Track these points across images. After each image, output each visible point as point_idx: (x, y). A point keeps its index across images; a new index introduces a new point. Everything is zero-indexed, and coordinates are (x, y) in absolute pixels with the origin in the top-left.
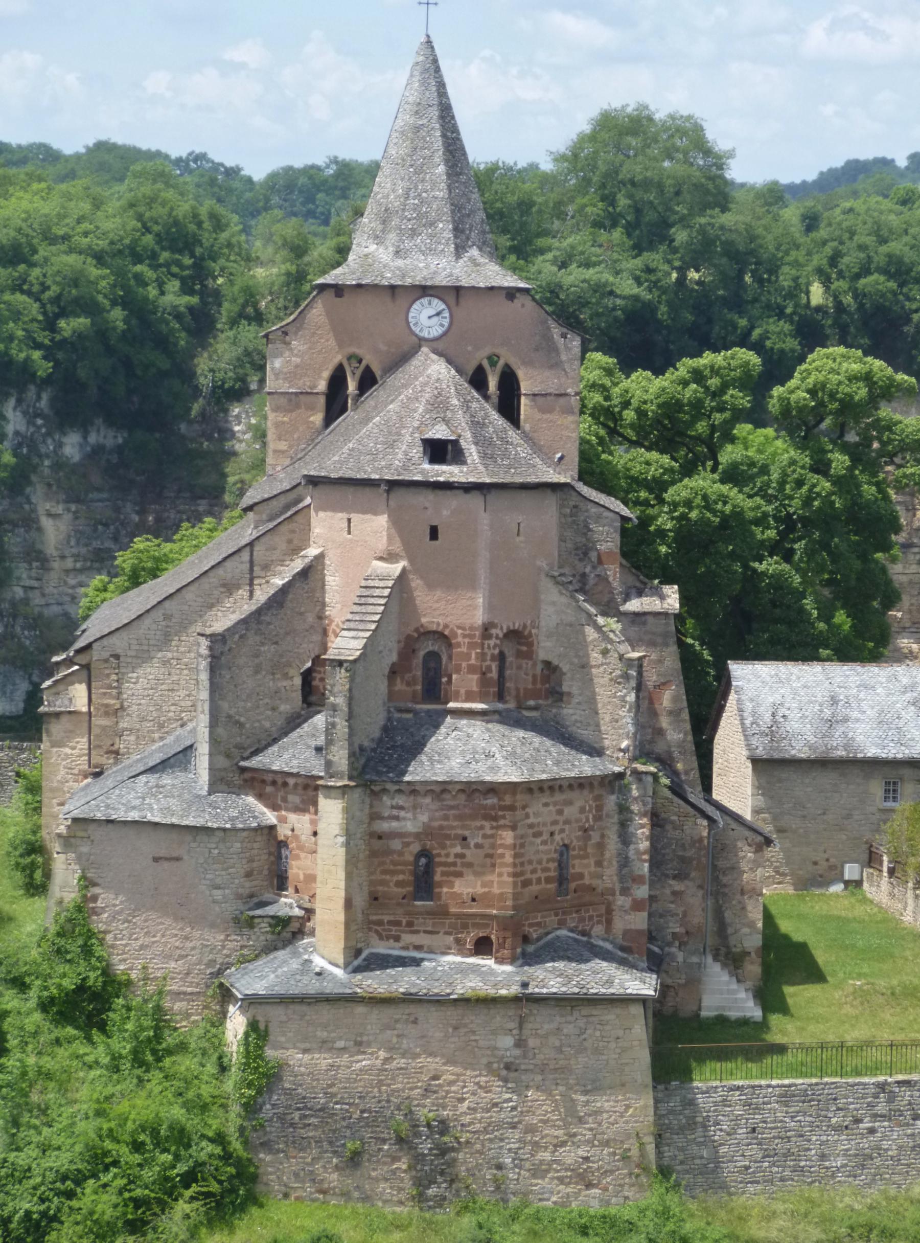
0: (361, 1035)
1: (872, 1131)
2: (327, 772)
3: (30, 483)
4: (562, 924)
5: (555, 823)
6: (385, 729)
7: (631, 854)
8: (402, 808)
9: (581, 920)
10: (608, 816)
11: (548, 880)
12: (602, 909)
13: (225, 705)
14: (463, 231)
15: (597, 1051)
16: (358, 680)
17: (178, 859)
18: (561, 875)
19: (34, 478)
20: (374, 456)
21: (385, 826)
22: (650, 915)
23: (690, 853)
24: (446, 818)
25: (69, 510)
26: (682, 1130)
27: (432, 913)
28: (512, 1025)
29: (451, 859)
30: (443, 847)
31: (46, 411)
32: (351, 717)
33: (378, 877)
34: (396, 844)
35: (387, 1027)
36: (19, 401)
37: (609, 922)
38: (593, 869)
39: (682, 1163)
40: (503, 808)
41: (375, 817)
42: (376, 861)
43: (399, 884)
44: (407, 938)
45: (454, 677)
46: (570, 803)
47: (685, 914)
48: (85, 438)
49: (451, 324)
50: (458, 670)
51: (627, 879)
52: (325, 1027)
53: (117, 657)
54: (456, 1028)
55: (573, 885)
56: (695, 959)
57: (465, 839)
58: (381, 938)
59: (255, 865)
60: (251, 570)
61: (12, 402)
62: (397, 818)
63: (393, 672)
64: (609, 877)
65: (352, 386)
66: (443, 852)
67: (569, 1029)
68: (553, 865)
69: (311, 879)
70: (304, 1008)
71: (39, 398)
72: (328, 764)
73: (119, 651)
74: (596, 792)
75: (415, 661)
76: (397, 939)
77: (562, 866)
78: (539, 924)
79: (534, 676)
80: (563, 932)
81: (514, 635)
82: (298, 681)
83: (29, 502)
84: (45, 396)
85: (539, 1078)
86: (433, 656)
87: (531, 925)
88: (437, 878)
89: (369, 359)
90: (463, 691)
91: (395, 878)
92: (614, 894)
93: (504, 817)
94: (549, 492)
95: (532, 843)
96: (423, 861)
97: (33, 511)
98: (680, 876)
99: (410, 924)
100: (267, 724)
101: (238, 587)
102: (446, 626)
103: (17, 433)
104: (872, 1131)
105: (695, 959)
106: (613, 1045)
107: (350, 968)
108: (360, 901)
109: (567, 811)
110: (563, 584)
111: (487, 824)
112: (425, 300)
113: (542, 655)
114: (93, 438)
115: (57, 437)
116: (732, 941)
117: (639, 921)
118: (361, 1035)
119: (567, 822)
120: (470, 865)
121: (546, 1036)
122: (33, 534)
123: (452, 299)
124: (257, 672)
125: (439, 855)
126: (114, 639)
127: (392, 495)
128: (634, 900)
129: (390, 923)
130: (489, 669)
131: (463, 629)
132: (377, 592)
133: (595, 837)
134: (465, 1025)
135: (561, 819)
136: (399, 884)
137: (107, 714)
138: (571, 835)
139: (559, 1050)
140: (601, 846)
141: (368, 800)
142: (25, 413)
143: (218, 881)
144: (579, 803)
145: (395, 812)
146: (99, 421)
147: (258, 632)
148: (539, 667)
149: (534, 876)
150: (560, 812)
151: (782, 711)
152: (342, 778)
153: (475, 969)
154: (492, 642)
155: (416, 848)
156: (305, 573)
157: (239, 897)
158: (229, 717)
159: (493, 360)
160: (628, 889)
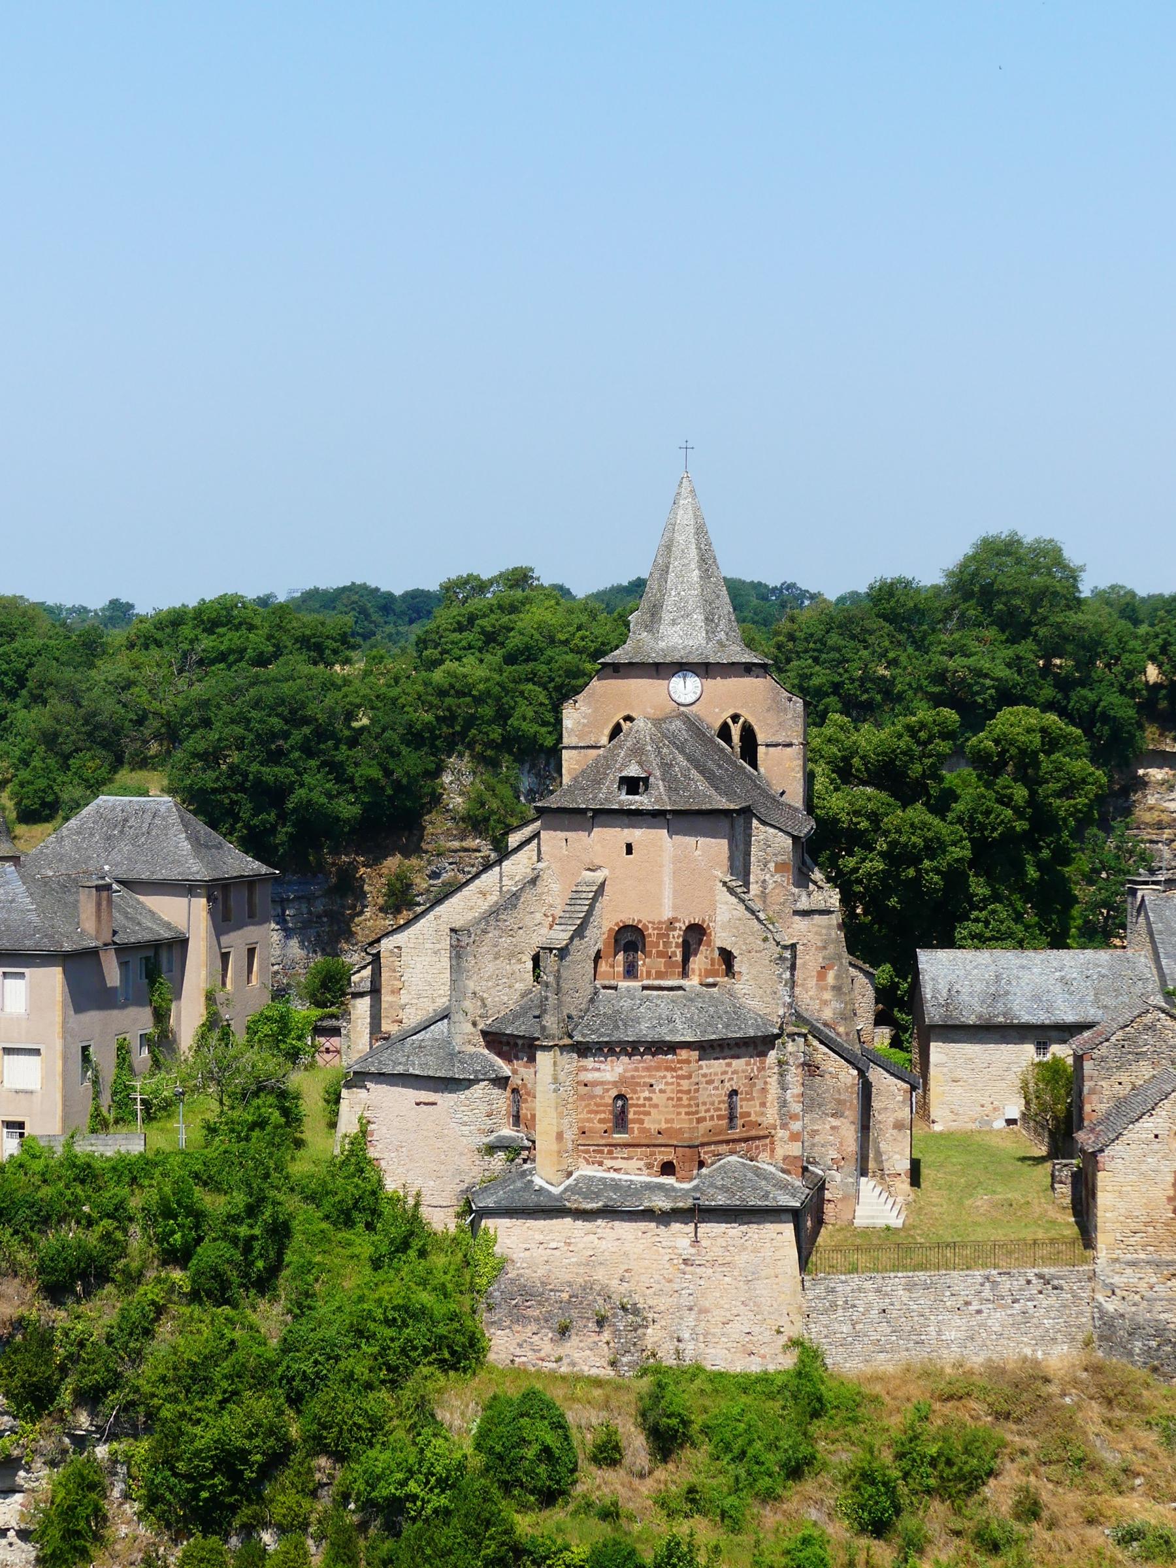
1: (979, 1312)
5: (725, 1073)
11: (720, 1117)
14: (712, 620)
15: (756, 1251)
17: (435, 1104)
23: (842, 1097)
24: (636, 1070)
29: (641, 1102)
30: (635, 1092)
33: (584, 1116)
34: (598, 1090)
37: (772, 1150)
38: (758, 1109)
39: (826, 1337)
43: (601, 1121)
44: (609, 1163)
47: (841, 1143)
53: (399, 948)
57: (651, 1086)
58: (588, 1163)
60: (501, 880)
61: (527, 766)
64: (771, 1116)
66: (635, 1096)
68: (724, 1106)
69: (533, 1116)
76: (601, 1164)
77: (732, 1107)
79: (712, 960)
88: (631, 1116)
90: (653, 971)
91: (598, 1117)
93: (681, 1068)
94: (722, 817)
96: (620, 1103)
102: (640, 921)
104: (979, 1312)
111: (669, 1074)
113: (719, 944)
116: (886, 1165)
118: (569, 1238)
120: (656, 1106)
124: (496, 958)
125: (632, 1098)
128: (792, 1133)
130: (674, 953)
131: (653, 923)
132: (584, 895)
133: (760, 1084)
135: (730, 1070)
136: (601, 1121)
137: (393, 992)
147: (497, 927)
149: (708, 1115)
151: (957, 987)
153: (660, 1187)
154: (676, 933)
155: (614, 1093)
159: (735, 718)
160: (787, 1124)
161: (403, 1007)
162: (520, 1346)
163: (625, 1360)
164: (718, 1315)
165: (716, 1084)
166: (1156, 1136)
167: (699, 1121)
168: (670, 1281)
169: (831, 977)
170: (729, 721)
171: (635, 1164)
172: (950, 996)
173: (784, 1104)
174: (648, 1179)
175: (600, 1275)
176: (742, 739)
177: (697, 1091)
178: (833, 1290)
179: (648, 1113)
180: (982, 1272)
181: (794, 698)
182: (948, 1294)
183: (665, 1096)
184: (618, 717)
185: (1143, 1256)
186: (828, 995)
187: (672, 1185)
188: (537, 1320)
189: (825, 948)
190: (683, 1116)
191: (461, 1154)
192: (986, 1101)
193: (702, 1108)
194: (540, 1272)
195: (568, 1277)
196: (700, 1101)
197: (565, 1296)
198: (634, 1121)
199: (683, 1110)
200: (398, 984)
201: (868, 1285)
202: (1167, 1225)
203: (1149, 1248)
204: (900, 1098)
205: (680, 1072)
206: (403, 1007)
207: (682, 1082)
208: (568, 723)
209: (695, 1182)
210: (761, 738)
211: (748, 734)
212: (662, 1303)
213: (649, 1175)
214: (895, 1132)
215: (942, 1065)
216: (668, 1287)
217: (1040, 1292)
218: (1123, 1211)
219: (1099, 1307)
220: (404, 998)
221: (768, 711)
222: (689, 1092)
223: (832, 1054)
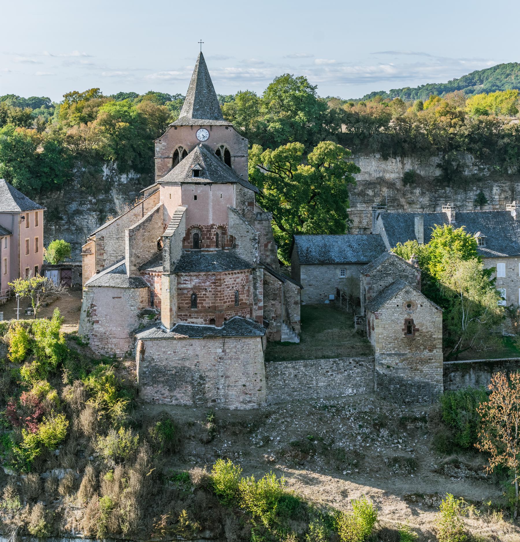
0: (175, 349)
2: (164, 270)
3: (111, 189)
4: (236, 314)
5: (234, 284)
6: (182, 257)
7: (257, 293)
8: (187, 280)
9: (243, 313)
10: (250, 281)
11: (232, 301)
12: (249, 309)
13: (134, 251)
15: (247, 353)
16: (173, 242)
17: (120, 298)
18: (236, 300)
19: (112, 188)
20: (177, 175)
21: (182, 286)
22: (264, 312)
23: (277, 292)
25: (123, 197)
26: (274, 376)
27: (196, 312)
28: (221, 345)
29: (202, 296)
30: (200, 292)
31: (116, 168)
32: (170, 253)
33: (180, 301)
34: (185, 292)
35: (183, 347)
36: (107, 166)
37: (251, 314)
40: (217, 280)
41: (179, 283)
42: (179, 297)
43: (186, 303)
45: (203, 241)
46: (238, 278)
47: (276, 311)
48: (127, 176)
49: (209, 136)
50: (203, 238)
51: (256, 300)
52: (164, 347)
53: (103, 237)
54: (204, 347)
55: (240, 303)
56: (279, 324)
59: (144, 299)
60: (143, 210)
61: (105, 166)
62: (185, 284)
63: (184, 240)
65: (180, 155)
67: (239, 346)
68: (233, 297)
69: (160, 302)
70: (158, 342)
71: (114, 165)
72: (164, 268)
73: (104, 236)
74: (246, 274)
75: (191, 237)
76: (186, 320)
78: (229, 315)
79: (227, 240)
80: (238, 317)
81: (222, 228)
82: (156, 243)
83: (111, 195)
84: (115, 164)
85: (230, 361)
86: (196, 234)
87: (227, 315)
88: (198, 301)
89: (185, 147)
92: (252, 305)
93: (217, 282)
94: (230, 184)
95: (227, 290)
96: (194, 296)
97: (112, 197)
98: (274, 299)
99: (190, 316)
100: (147, 256)
101: (139, 215)
102: (200, 226)
103: (107, 175)
105: (279, 324)
106: (252, 351)
107: (172, 330)
108: (175, 309)
109: (237, 280)
110: (235, 212)
111: (212, 285)
112: (201, 130)
114: (130, 176)
115: (119, 176)
116: (291, 318)
117: (261, 313)
118: (175, 349)
119: (237, 284)
120: (208, 297)
121: (231, 349)
122: (112, 205)
123: (209, 129)
124: (144, 241)
126: (102, 232)
127: (183, 186)
128: (259, 307)
129: (184, 315)
132: (178, 216)
133: (246, 288)
134: (207, 346)
136: (186, 303)
138: (239, 287)
139: (236, 353)
140: (248, 291)
141: (176, 278)
142: (109, 169)
143: (132, 304)
144: (242, 278)
145: (185, 282)
146: (132, 171)
148: (229, 237)
149: (228, 300)
150: (235, 281)
151: (310, 249)
152: (168, 272)
153: (210, 329)
154: (214, 230)
155: (191, 292)
156: (158, 211)
157: (139, 309)
158: (135, 254)
159: (222, 147)
161: (104, 260)
162: (156, 393)
163: (197, 397)
164: (232, 379)
165: (230, 288)
166: (398, 306)
167: (225, 302)
168: (214, 366)
169: (269, 247)
170: (220, 148)
171: (200, 320)
172: (307, 253)
174: (205, 326)
175: (187, 364)
176: (225, 155)
177: (223, 291)
178: (276, 368)
179: (205, 300)
180: (333, 360)
181: (245, 139)
182: (320, 368)
183: (211, 293)
184: (177, 147)
185: (393, 352)
186: (268, 253)
187: (214, 328)
188: (163, 382)
189: (267, 235)
190: (218, 301)
191: (131, 317)
192: (322, 293)
193: (226, 298)
194: (164, 363)
195: (176, 365)
196: (224, 295)
197: (173, 372)
198: (200, 303)
199: (218, 299)
200: (102, 251)
201: (290, 365)
202: (402, 340)
203: (396, 349)
204: (296, 293)
205: (217, 284)
206: (104, 260)
207: (218, 288)
208: (157, 149)
209: (223, 326)
210: (232, 154)
211: (227, 153)
212: (211, 374)
213: (205, 324)
214: (294, 306)
215: (305, 279)
216: (213, 368)
217: (355, 367)
218: (385, 335)
219: (377, 372)
220: (105, 257)
221: (235, 144)
222: (220, 291)
223: (272, 276)
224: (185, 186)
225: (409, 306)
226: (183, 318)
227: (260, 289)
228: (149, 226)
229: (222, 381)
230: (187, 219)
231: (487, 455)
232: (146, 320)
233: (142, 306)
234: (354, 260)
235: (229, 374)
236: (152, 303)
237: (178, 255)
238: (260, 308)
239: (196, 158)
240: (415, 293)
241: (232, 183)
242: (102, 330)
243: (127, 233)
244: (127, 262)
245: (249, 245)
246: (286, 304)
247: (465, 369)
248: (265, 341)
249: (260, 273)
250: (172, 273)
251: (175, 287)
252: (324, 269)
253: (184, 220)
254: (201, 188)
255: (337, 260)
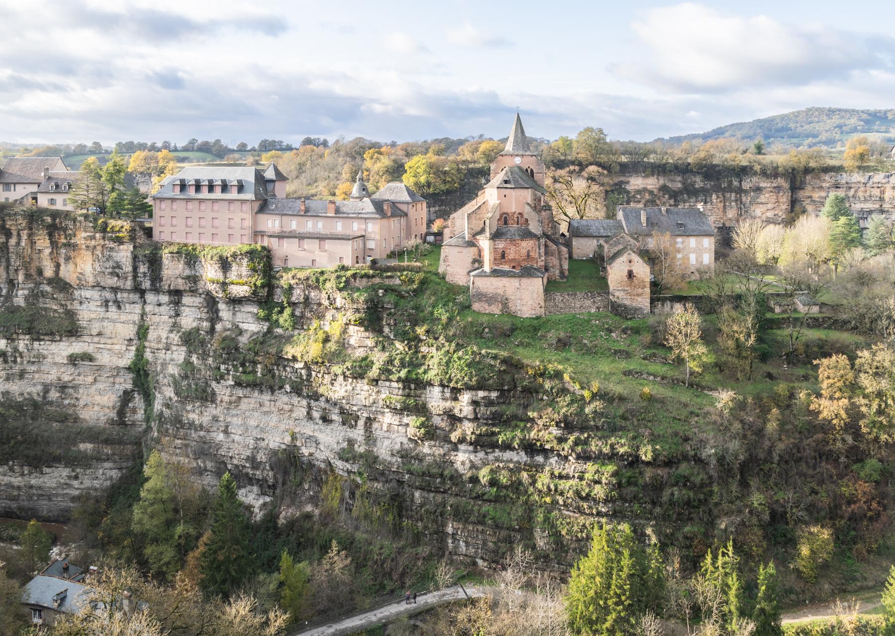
77: (528, 254)
81: (520, 214)
86: (506, 217)
108: (492, 259)
138: (530, 248)
173: (540, 253)
175: (499, 291)
211: (532, 171)
212: (513, 298)
220: (455, 229)
224: (499, 189)
225: (630, 262)
226: (498, 265)
227: (542, 250)
228: (479, 212)
229: (519, 302)
230: (500, 208)
231: (671, 348)
232: (476, 265)
233: (474, 257)
234: (605, 234)
235: (523, 298)
236: (480, 256)
237: (494, 229)
238: (542, 261)
239: (507, 173)
240: (633, 254)
241: (527, 188)
242: (452, 270)
243: (466, 215)
244: (466, 232)
245: (536, 224)
246: (560, 259)
247: (664, 300)
248: (545, 280)
249: (543, 241)
250: (490, 239)
251: (492, 247)
252: (586, 239)
253: (498, 208)
254: (509, 190)
255: (595, 234)
